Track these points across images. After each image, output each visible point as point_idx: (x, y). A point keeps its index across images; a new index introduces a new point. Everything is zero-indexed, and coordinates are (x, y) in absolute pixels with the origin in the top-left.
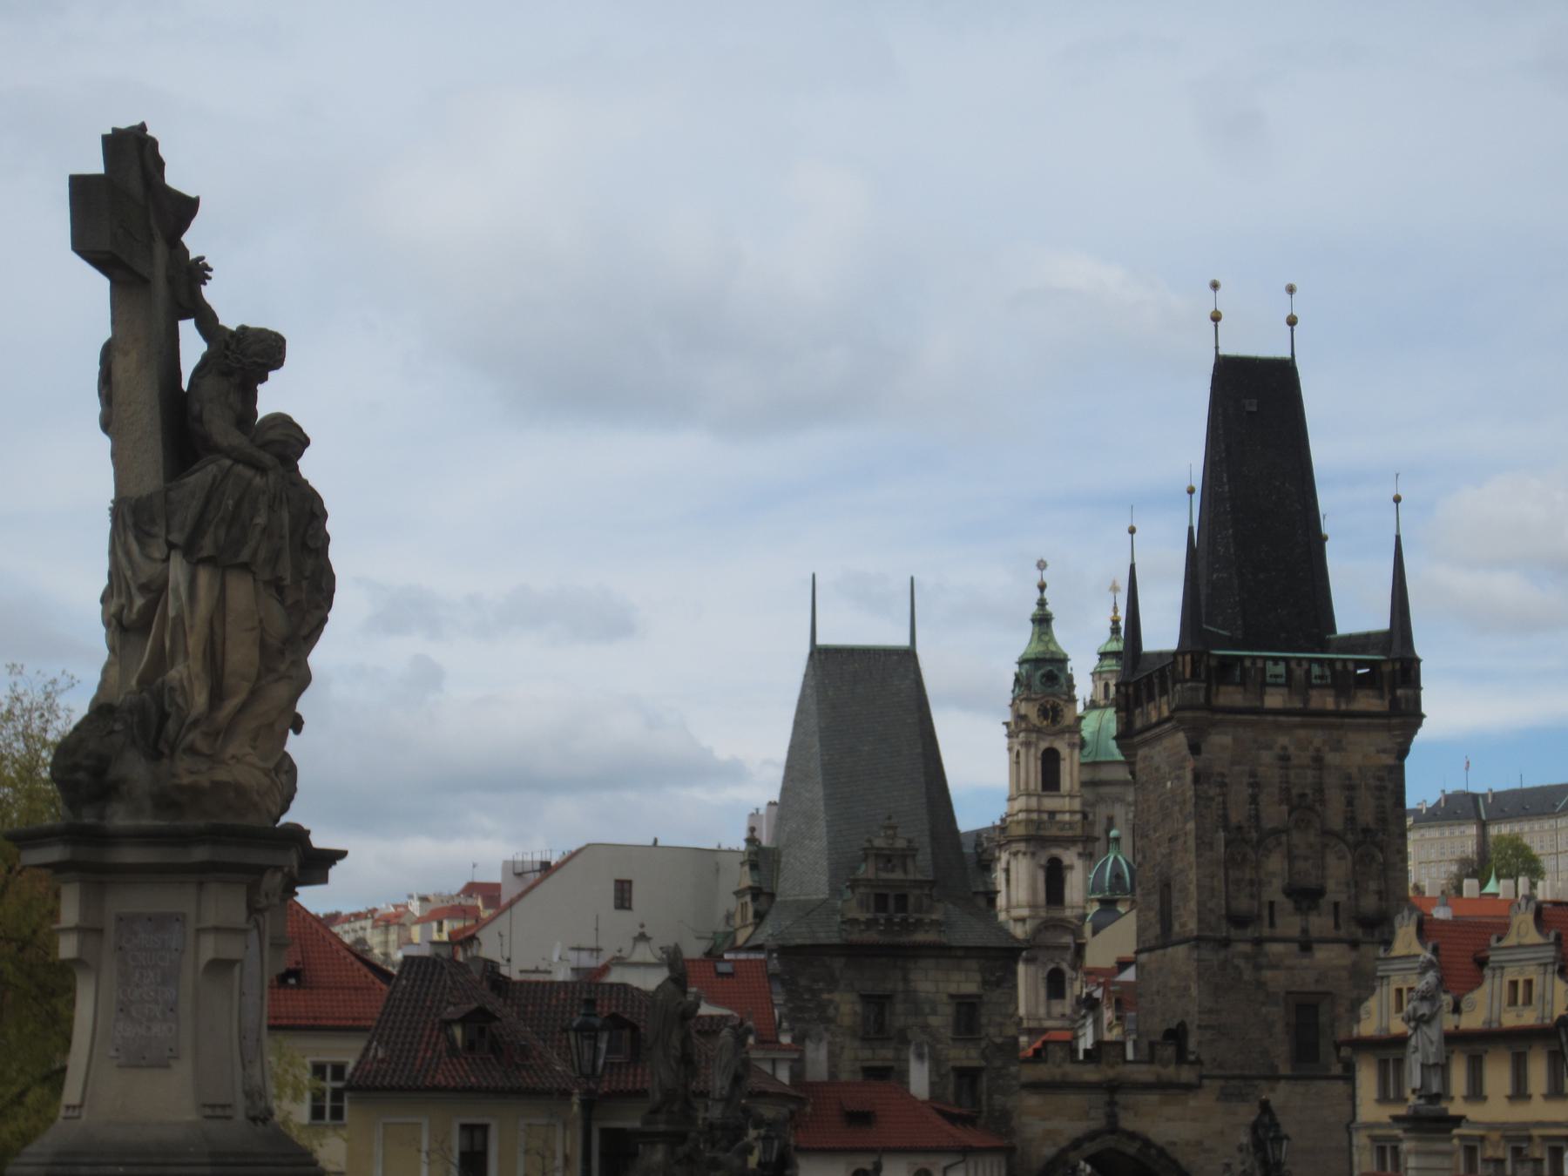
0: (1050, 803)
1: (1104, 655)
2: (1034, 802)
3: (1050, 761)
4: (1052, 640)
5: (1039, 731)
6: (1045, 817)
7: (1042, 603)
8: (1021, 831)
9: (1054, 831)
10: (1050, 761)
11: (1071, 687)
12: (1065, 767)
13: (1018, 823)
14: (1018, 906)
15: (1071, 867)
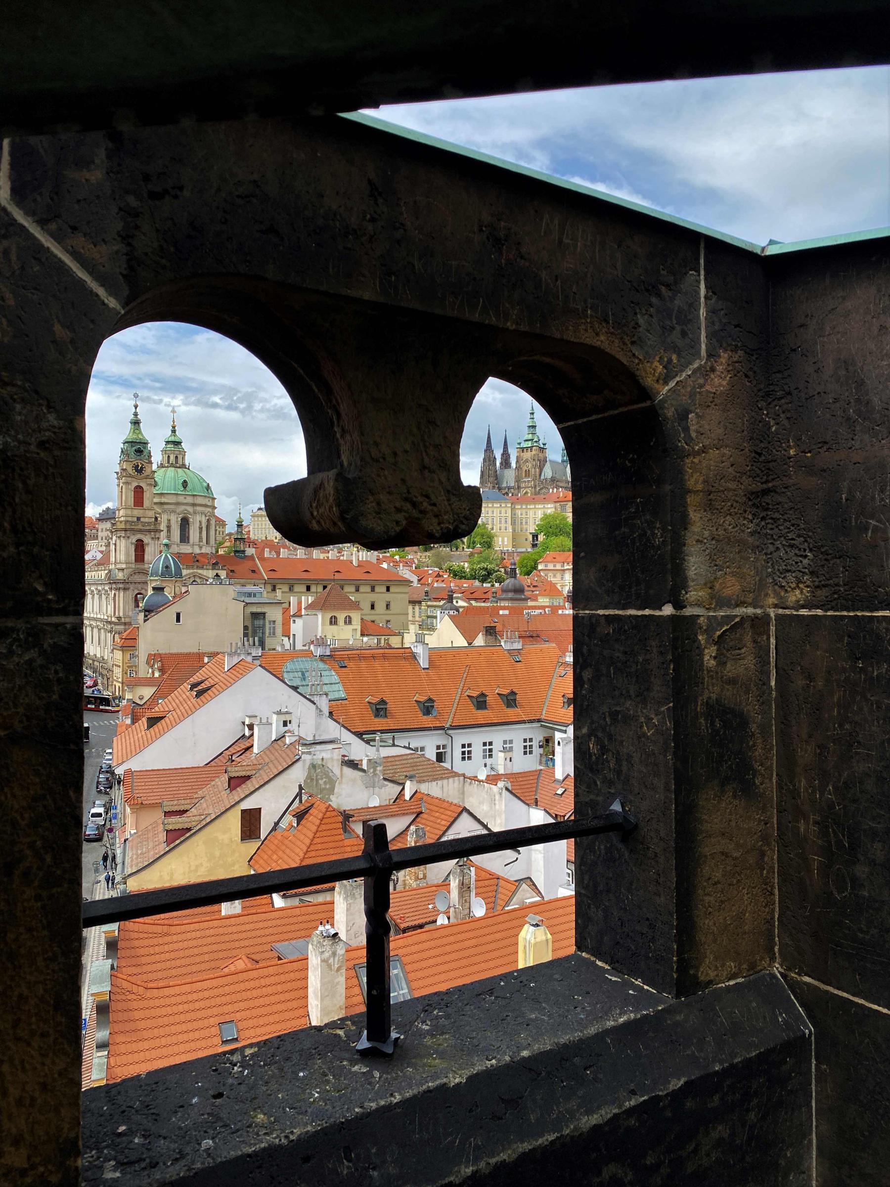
0: (137, 512)
1: (168, 442)
2: (129, 512)
3: (139, 492)
4: (140, 433)
5: (131, 476)
6: (135, 519)
7: (136, 414)
8: (123, 526)
9: (140, 527)
10: (139, 492)
11: (150, 456)
12: (147, 495)
13: (121, 522)
14: (120, 563)
15: (148, 544)
